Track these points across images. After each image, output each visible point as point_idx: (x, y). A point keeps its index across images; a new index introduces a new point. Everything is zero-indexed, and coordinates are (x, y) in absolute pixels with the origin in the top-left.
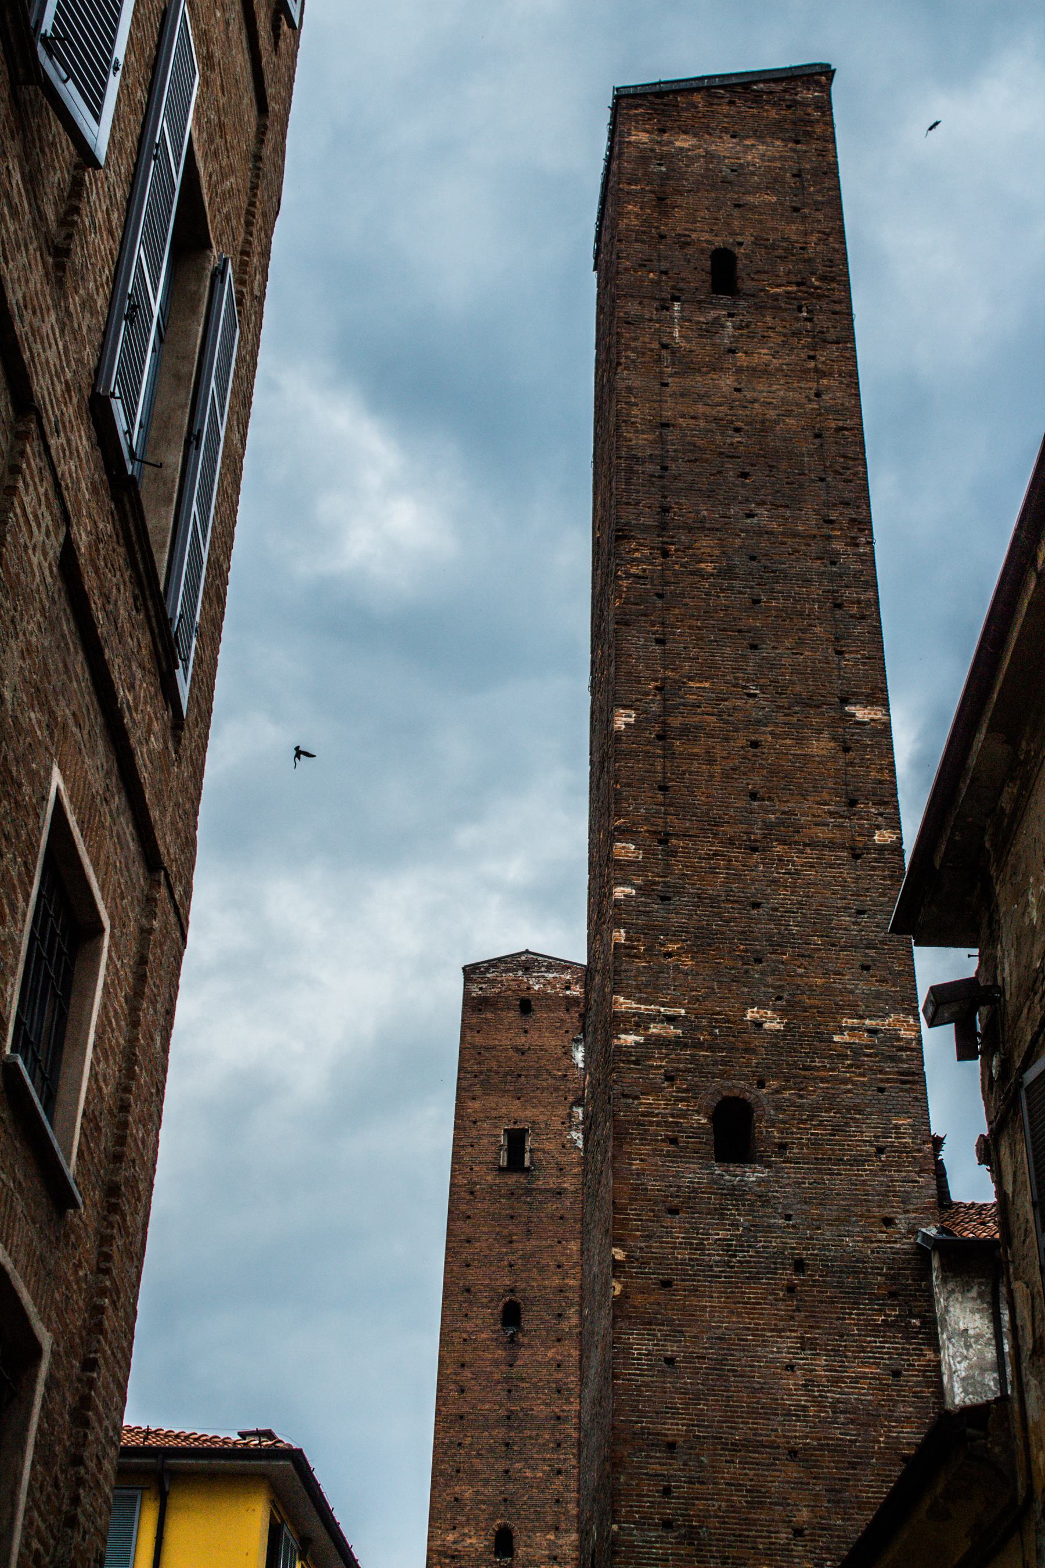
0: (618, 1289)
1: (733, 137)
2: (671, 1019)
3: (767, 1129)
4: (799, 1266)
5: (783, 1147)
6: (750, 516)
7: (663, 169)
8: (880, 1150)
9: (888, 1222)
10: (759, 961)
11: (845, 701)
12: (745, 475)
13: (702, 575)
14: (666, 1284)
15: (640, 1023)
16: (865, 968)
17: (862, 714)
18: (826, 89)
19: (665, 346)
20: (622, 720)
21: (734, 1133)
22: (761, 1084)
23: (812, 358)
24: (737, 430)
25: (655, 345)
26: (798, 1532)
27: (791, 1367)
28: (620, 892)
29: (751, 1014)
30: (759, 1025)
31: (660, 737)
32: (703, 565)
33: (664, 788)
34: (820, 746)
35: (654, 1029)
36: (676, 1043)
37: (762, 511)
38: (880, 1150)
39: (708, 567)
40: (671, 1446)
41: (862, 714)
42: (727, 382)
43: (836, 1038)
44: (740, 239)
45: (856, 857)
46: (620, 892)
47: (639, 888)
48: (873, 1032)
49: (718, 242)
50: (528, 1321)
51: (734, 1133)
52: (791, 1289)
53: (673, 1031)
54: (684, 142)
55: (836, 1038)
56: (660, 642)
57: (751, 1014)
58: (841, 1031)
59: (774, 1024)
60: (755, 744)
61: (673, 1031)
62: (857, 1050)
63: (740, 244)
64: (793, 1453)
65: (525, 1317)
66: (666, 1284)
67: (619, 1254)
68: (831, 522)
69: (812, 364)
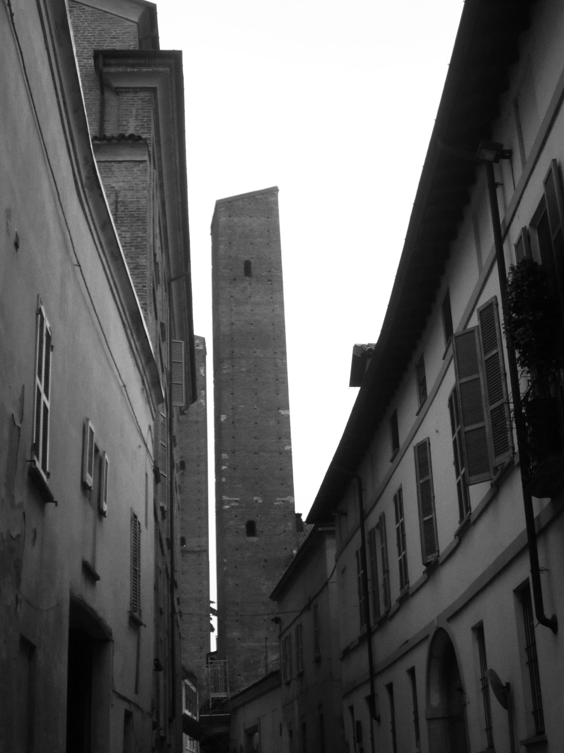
0: (225, 569)
1: (250, 217)
2: (236, 501)
3: (258, 528)
4: (266, 561)
5: (262, 532)
6: (255, 352)
7: (230, 231)
8: (285, 531)
9: (286, 549)
10: (257, 484)
11: (279, 409)
12: (253, 339)
13: (242, 372)
14: (236, 567)
15: (229, 502)
16: (282, 484)
17: (283, 412)
18: (276, 196)
19: (232, 297)
20: (223, 418)
21: (251, 529)
22: (257, 516)
23: (272, 298)
24: (252, 324)
25: (229, 296)
26: (265, 621)
27: (263, 584)
28: (224, 467)
29: (255, 498)
30: (257, 501)
31: (233, 423)
32: (242, 369)
33: (234, 438)
34: (272, 423)
35: (233, 504)
36: (238, 507)
37: (258, 351)
38: (285, 531)
39: (244, 369)
40: (238, 604)
41: (283, 412)
42: (248, 308)
43: (275, 504)
44: (252, 256)
45: (281, 454)
46: (224, 467)
47: (227, 466)
48: (283, 501)
49: (247, 258)
50: (188, 466)
51: (251, 529)
52: (264, 566)
53: (237, 504)
54: (236, 220)
55: (275, 504)
56: (232, 394)
57: (255, 498)
58: (276, 501)
59: (260, 501)
60: (256, 423)
61: (237, 504)
62: (280, 506)
63: (252, 258)
64: (264, 603)
65: (186, 466)
66: (236, 567)
67: (225, 561)
68: (276, 353)
69: (271, 300)
